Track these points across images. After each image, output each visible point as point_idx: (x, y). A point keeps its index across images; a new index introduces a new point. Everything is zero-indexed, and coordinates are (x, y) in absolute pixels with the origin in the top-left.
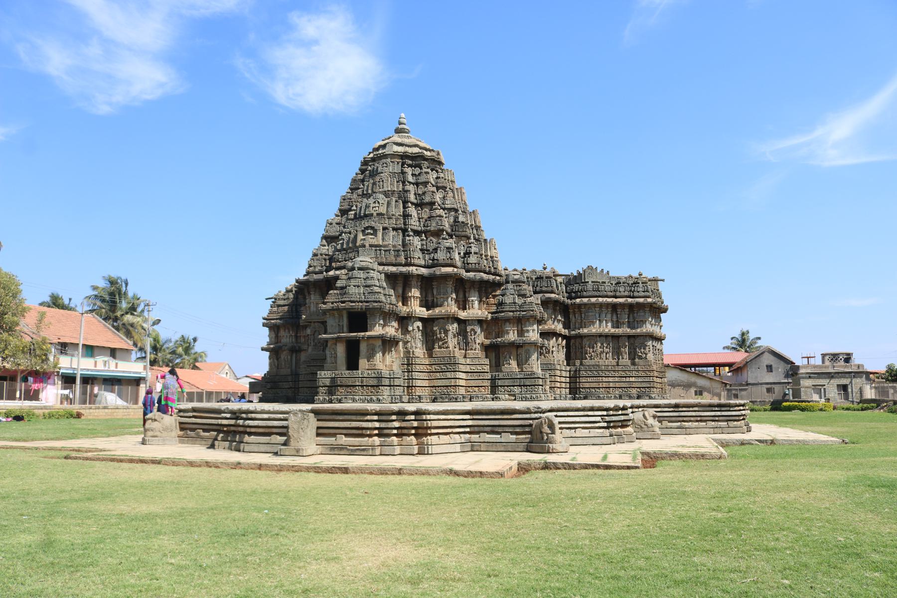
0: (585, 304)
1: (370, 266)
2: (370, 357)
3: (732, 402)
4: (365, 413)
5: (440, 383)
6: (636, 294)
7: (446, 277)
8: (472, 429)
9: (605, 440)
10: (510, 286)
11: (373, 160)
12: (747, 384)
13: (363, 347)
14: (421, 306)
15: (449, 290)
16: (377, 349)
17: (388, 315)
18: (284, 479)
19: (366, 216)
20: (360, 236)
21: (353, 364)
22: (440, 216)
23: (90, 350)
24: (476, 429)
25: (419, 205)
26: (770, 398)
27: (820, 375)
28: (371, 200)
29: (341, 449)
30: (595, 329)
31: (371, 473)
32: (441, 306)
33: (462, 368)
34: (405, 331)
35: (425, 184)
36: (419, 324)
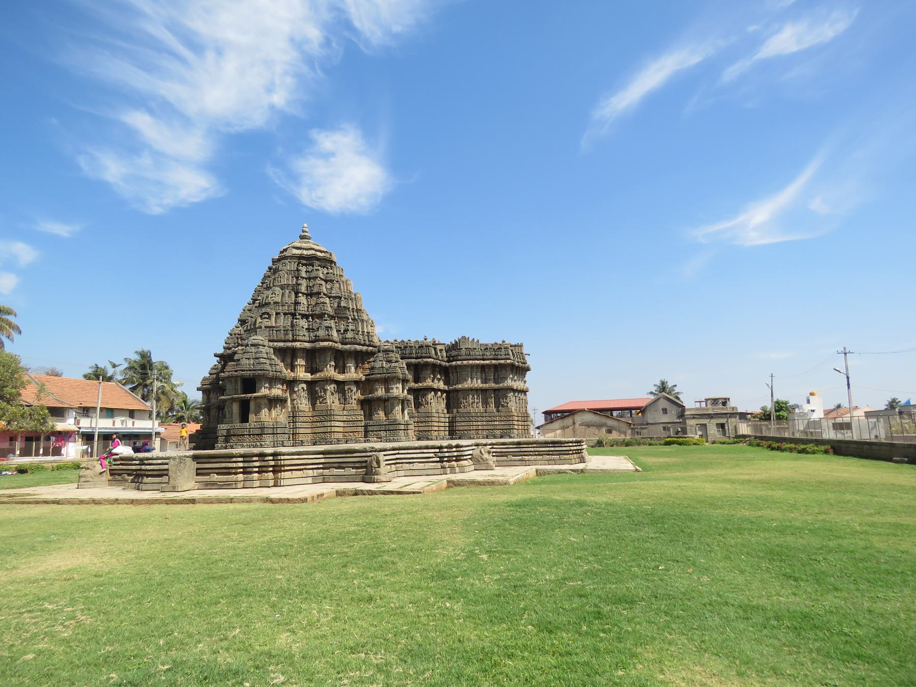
0: (460, 366)
1: (261, 342)
2: (257, 412)
4: (231, 456)
6: (499, 357)
7: (324, 349)
9: (436, 472)
10: (380, 354)
11: (279, 260)
12: (647, 424)
13: (252, 405)
14: (306, 372)
17: (273, 381)
18: (142, 510)
20: (259, 320)
23: (109, 412)
24: (328, 465)
25: (309, 295)
28: (270, 292)
30: (468, 384)
31: (211, 503)
33: (339, 418)
34: (292, 392)
36: (304, 386)
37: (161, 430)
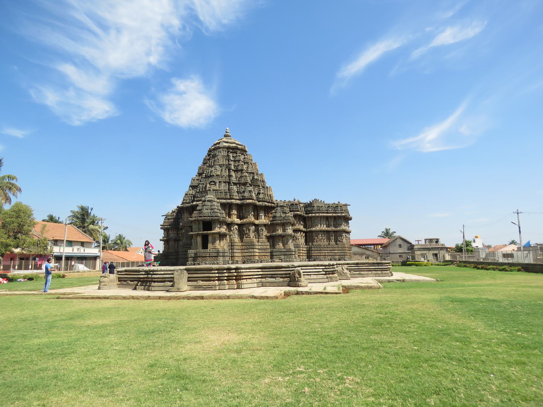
0: (314, 217)
1: (213, 199)
2: (213, 243)
3: (383, 262)
5: (247, 254)
6: (337, 212)
8: (262, 276)
10: (279, 208)
11: (214, 149)
12: (390, 254)
13: (210, 238)
15: (250, 211)
16: (217, 239)
17: (222, 223)
18: (172, 304)
19: (211, 176)
20: (208, 186)
21: (205, 246)
22: (246, 176)
23: (70, 243)
24: (264, 276)
25: (236, 171)
26: (401, 260)
27: (424, 249)
28: (213, 169)
29: (200, 287)
30: (318, 228)
31: (215, 299)
32: (247, 218)
33: (257, 247)
34: (230, 230)
35: (239, 161)
36: (237, 227)
37: (102, 254)
